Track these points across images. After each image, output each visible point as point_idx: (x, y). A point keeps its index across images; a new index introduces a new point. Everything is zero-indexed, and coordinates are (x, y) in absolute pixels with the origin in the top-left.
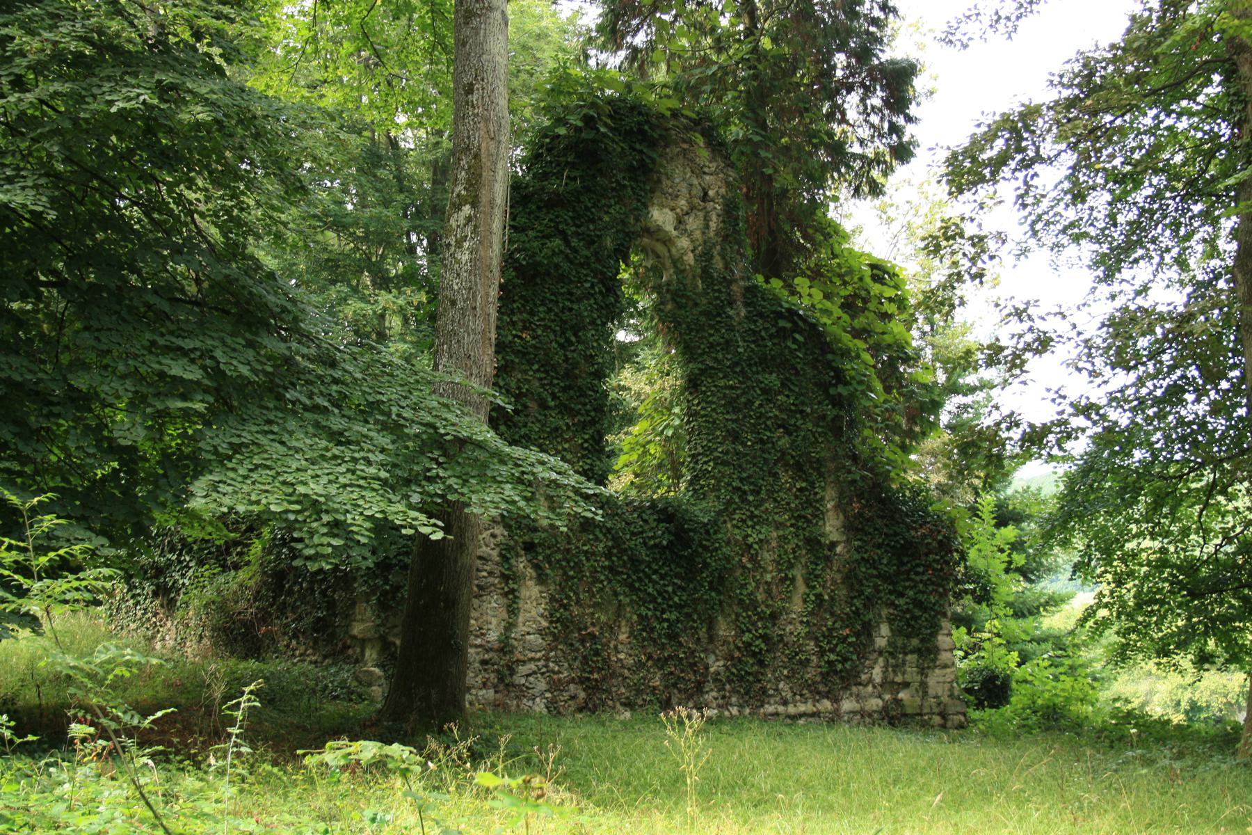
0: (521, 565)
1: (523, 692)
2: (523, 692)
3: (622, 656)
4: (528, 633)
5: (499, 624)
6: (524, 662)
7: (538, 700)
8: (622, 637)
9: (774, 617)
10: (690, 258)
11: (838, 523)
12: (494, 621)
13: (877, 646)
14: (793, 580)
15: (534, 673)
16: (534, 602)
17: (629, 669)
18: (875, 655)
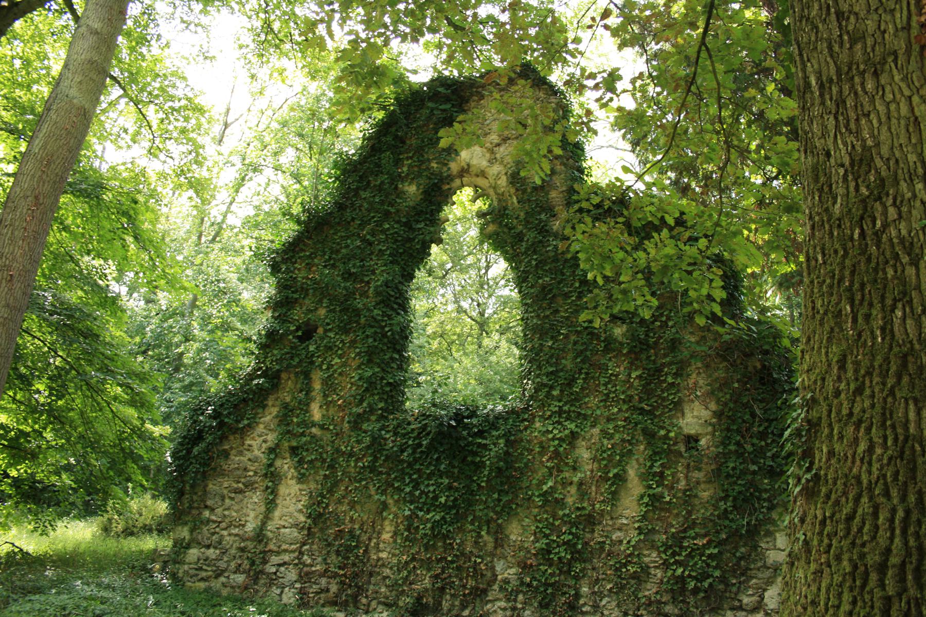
0: (286, 467)
1: (273, 580)
2: (273, 580)
3: (384, 555)
4: (284, 527)
5: (256, 517)
6: (278, 553)
7: (287, 589)
8: (386, 536)
9: (591, 521)
10: (503, 182)
11: (706, 414)
12: (252, 514)
13: (770, 561)
14: (621, 478)
15: (285, 563)
16: (293, 501)
17: (391, 568)
18: (768, 573)
